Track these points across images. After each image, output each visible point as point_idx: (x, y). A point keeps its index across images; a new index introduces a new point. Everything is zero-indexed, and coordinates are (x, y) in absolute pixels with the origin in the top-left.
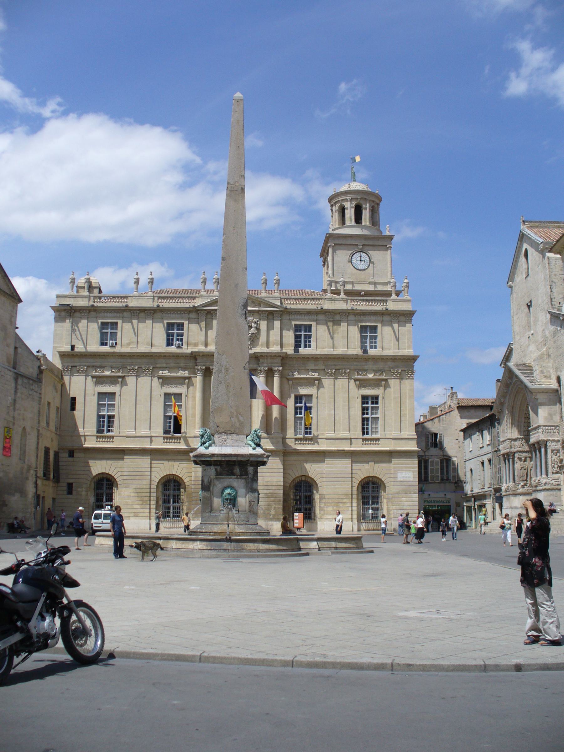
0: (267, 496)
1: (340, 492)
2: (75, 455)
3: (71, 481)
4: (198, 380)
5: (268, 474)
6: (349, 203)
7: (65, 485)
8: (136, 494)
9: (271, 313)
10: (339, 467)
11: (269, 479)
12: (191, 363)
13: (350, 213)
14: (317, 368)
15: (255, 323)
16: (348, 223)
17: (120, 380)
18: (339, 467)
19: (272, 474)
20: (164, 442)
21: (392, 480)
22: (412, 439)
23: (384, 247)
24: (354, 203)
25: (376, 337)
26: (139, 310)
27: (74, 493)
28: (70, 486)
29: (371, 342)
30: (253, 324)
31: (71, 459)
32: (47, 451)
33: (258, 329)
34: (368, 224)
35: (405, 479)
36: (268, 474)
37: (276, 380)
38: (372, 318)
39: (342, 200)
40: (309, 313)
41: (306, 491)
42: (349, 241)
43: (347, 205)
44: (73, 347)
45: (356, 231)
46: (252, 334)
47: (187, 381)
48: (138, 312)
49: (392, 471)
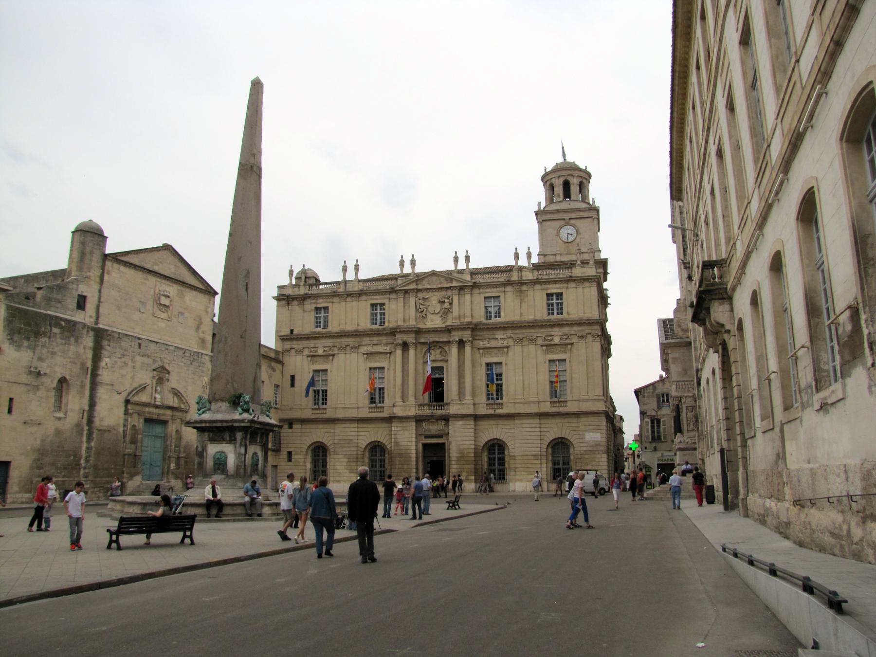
0: (459, 459)
9: (461, 288)
11: (461, 443)
12: (390, 339)
13: (559, 190)
14: (505, 336)
15: (448, 298)
17: (328, 356)
19: (465, 439)
21: (578, 440)
22: (599, 400)
24: (562, 180)
25: (562, 304)
28: (290, 454)
29: (558, 309)
30: (446, 301)
33: (451, 304)
38: (558, 286)
40: (497, 285)
41: (499, 453)
42: (556, 216)
44: (292, 331)
45: (565, 205)
49: (581, 432)
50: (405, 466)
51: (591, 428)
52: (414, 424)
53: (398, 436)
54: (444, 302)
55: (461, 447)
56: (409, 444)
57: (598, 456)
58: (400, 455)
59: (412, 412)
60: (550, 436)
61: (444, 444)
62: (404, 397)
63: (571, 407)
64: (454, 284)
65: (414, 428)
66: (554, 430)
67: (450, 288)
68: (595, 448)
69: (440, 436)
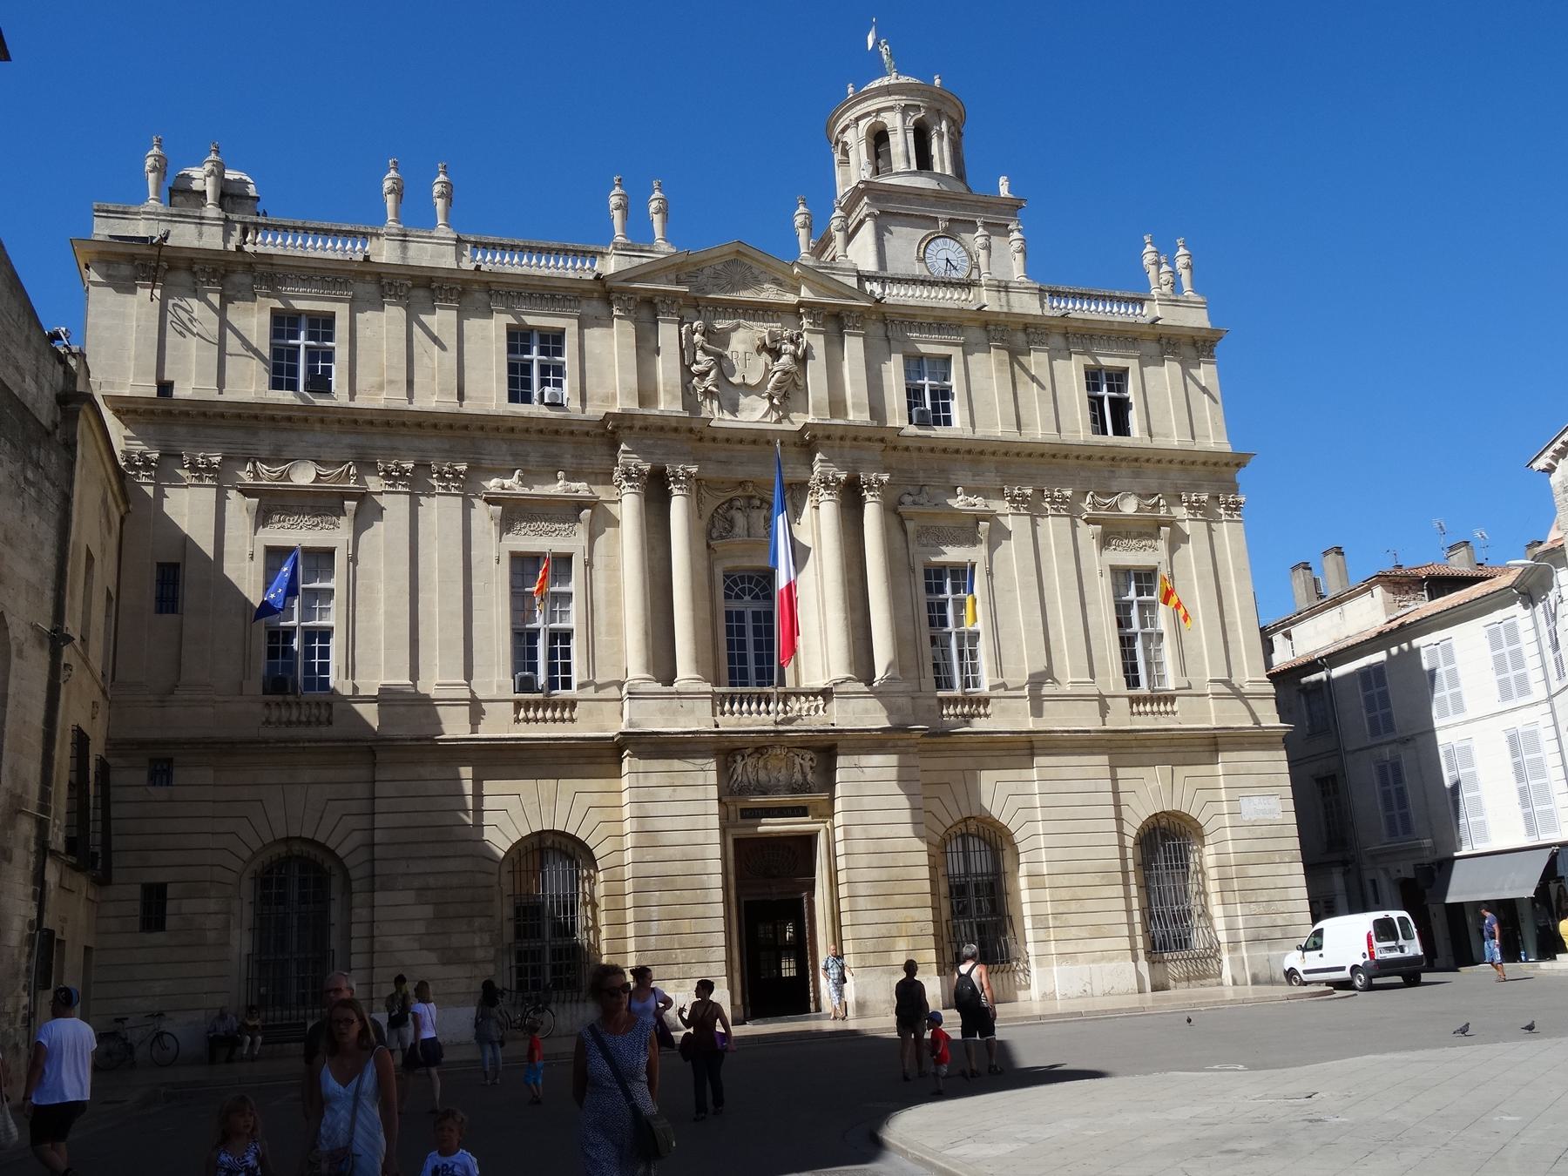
1: (1088, 866)
2: (179, 775)
3: (158, 877)
4: (628, 507)
5: (877, 817)
6: (899, 116)
7: (136, 892)
8: (428, 911)
10: (1076, 786)
16: (899, 164)
18: (1076, 786)
20: (517, 720)
23: (1002, 230)
26: (412, 277)
27: (170, 922)
31: (160, 792)
32: (81, 740)
34: (948, 172)
35: (1261, 816)
36: (877, 817)
37: (872, 514)
39: (879, 111)
43: (893, 121)
46: (786, 373)
47: (587, 512)
48: (410, 283)
50: (686, 926)
51: (1252, 780)
52: (712, 764)
53: (652, 809)
54: (776, 354)
55: (887, 845)
56: (699, 837)
57: (1283, 869)
58: (666, 882)
59: (696, 719)
60: (1138, 814)
61: (809, 840)
62: (662, 664)
63: (1187, 717)
64: (806, 293)
65: (713, 777)
66: (1152, 791)
67: (795, 311)
68: (1270, 845)
69: (801, 811)
